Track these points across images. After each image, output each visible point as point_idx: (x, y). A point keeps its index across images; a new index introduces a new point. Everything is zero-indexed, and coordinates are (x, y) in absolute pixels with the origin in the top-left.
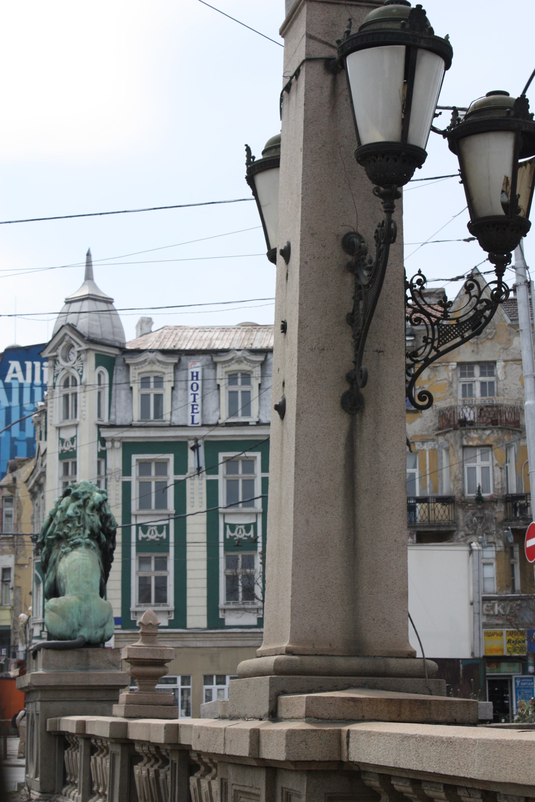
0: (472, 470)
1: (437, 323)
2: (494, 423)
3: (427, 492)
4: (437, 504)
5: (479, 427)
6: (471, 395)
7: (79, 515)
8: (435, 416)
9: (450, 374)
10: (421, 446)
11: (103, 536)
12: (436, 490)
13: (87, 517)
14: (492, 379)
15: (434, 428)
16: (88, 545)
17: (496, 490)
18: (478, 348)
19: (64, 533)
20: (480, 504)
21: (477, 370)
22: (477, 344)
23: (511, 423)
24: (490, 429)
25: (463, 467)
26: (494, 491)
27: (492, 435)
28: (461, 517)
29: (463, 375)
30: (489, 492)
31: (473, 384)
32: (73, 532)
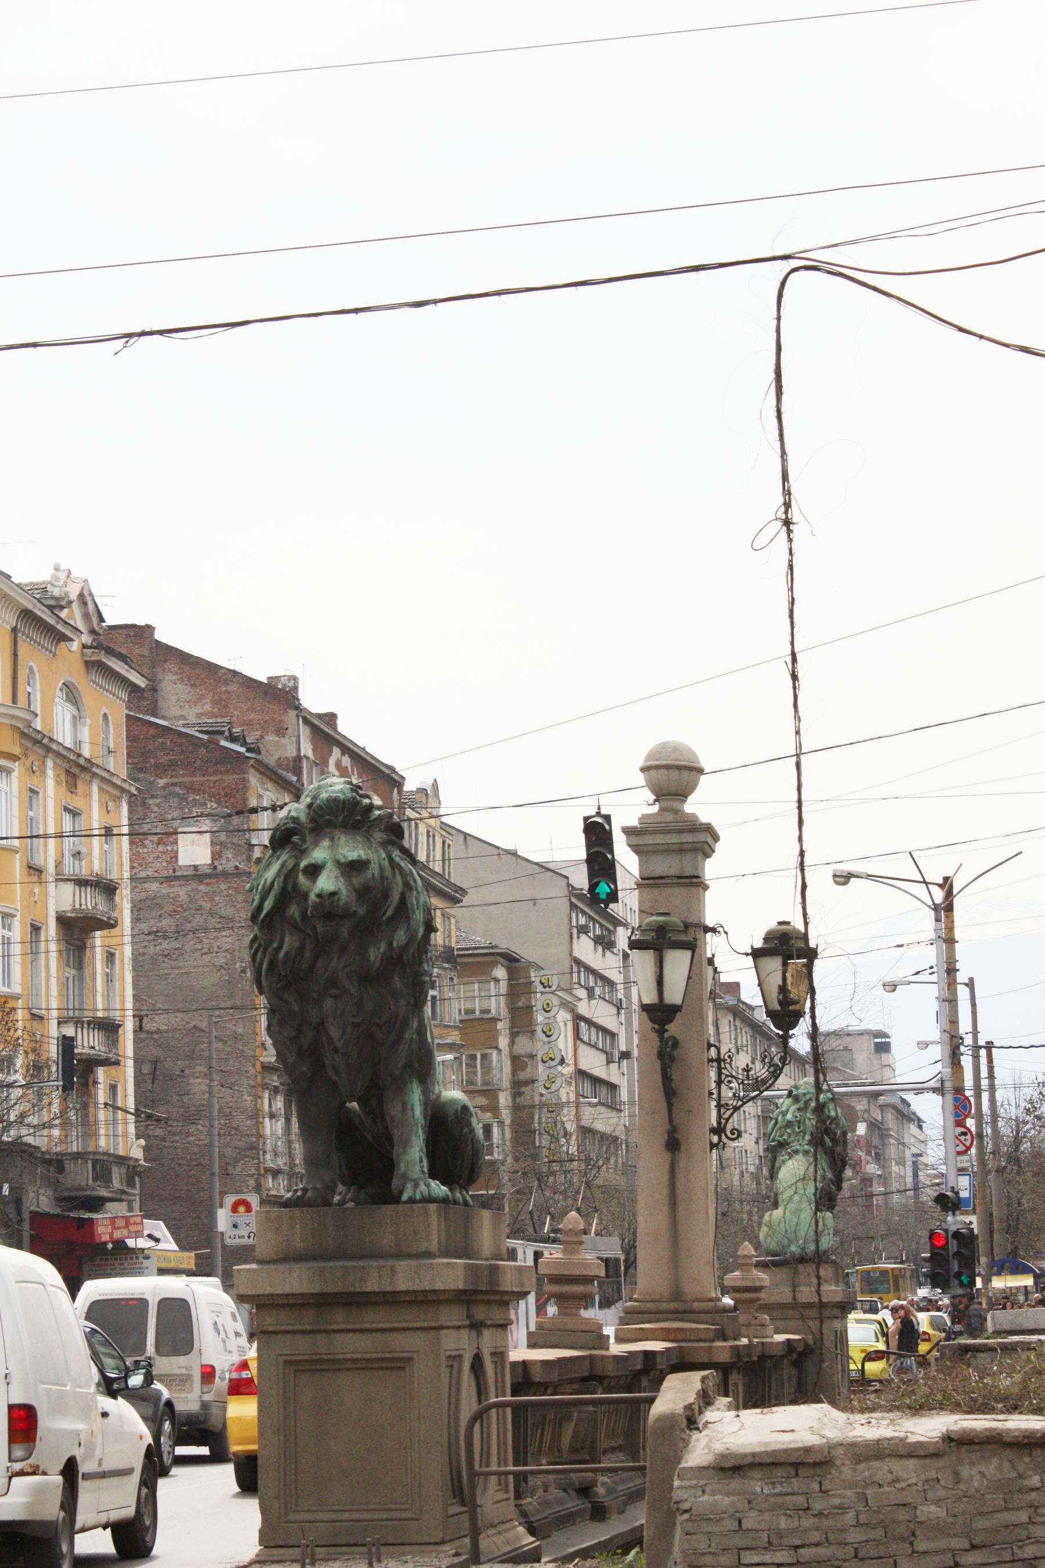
1: (742, 1083)
11: (827, 1140)
13: (807, 1121)
16: (806, 1153)
32: (792, 1138)
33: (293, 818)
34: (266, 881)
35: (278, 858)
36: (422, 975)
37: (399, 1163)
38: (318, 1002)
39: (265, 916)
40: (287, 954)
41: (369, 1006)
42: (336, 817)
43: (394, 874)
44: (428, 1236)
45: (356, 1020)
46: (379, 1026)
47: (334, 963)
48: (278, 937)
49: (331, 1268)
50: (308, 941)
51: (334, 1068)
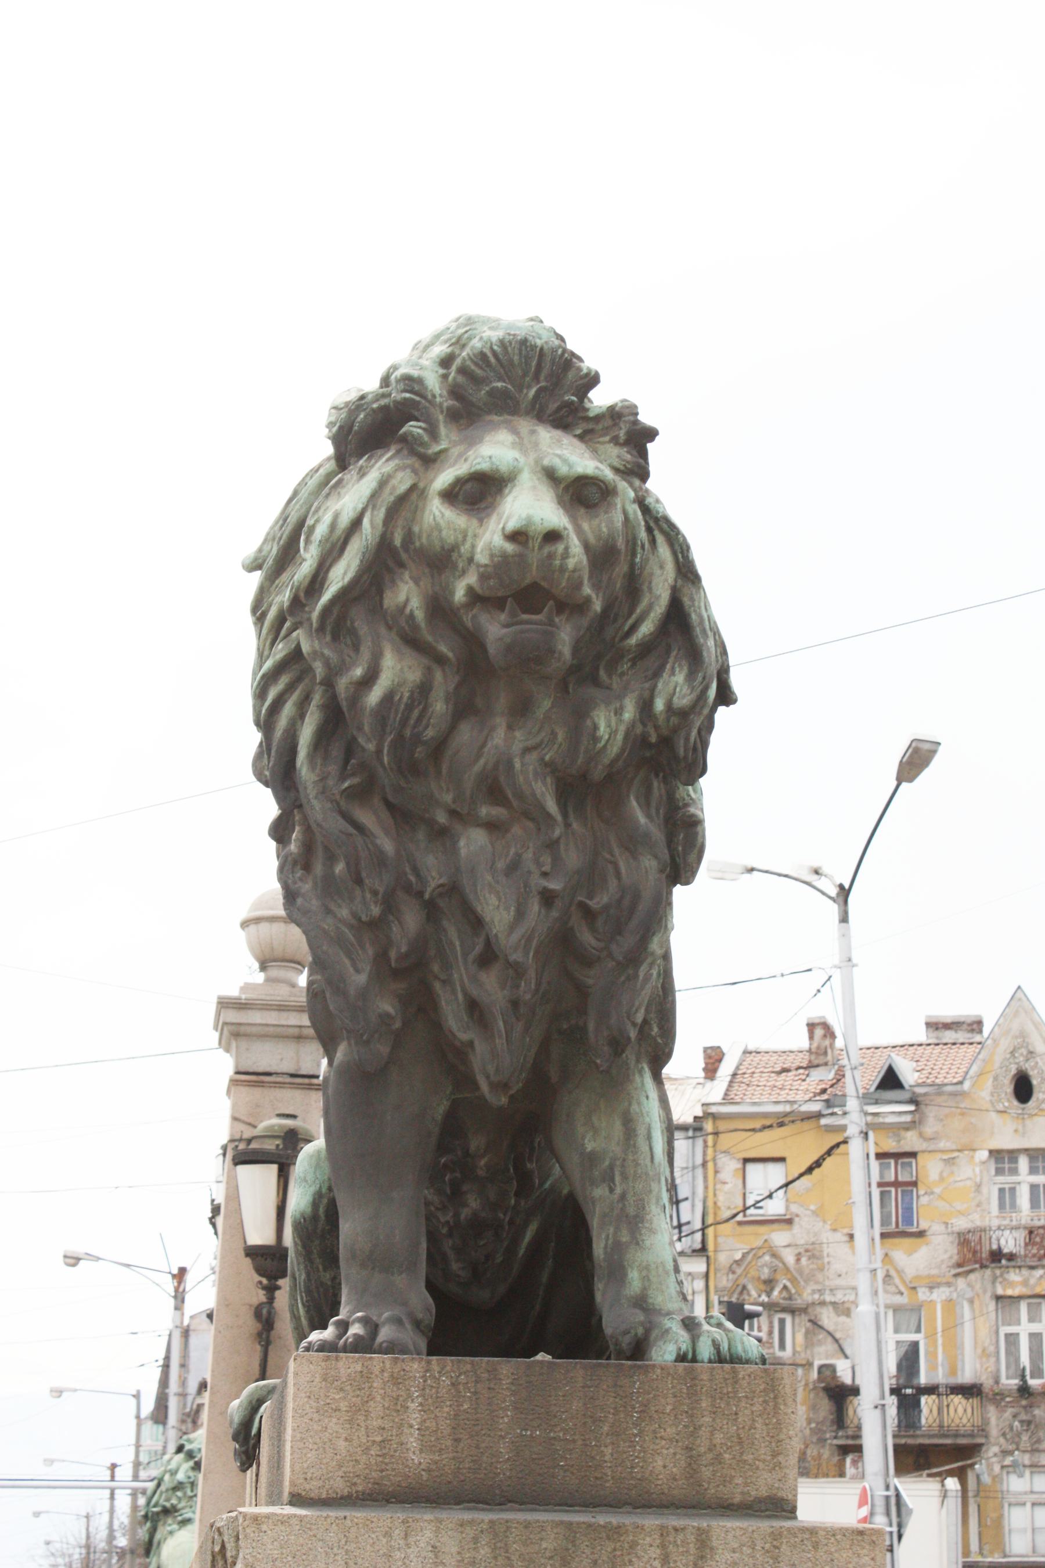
0: (1012, 1340)
3: (938, 1376)
4: (952, 1396)
5: (1023, 1263)
6: (1013, 1205)
7: (191, 1480)
8: (952, 1243)
9: (977, 1170)
10: (928, 1294)
12: (953, 1371)
15: (950, 1264)
18: (1024, 1126)
19: (172, 1504)
20: (1026, 1399)
21: (1023, 1163)
25: (997, 1332)
28: (993, 1421)
29: (999, 1172)
33: (407, 379)
34: (336, 516)
35: (362, 473)
36: (686, 805)
37: (618, 1272)
38: (441, 835)
39: (333, 602)
40: (388, 698)
41: (573, 858)
42: (520, 388)
43: (653, 541)
44: (775, 1454)
45: (555, 885)
46: (589, 915)
47: (499, 737)
48: (365, 654)
49: (527, 1525)
50: (438, 676)
51: (474, 1008)
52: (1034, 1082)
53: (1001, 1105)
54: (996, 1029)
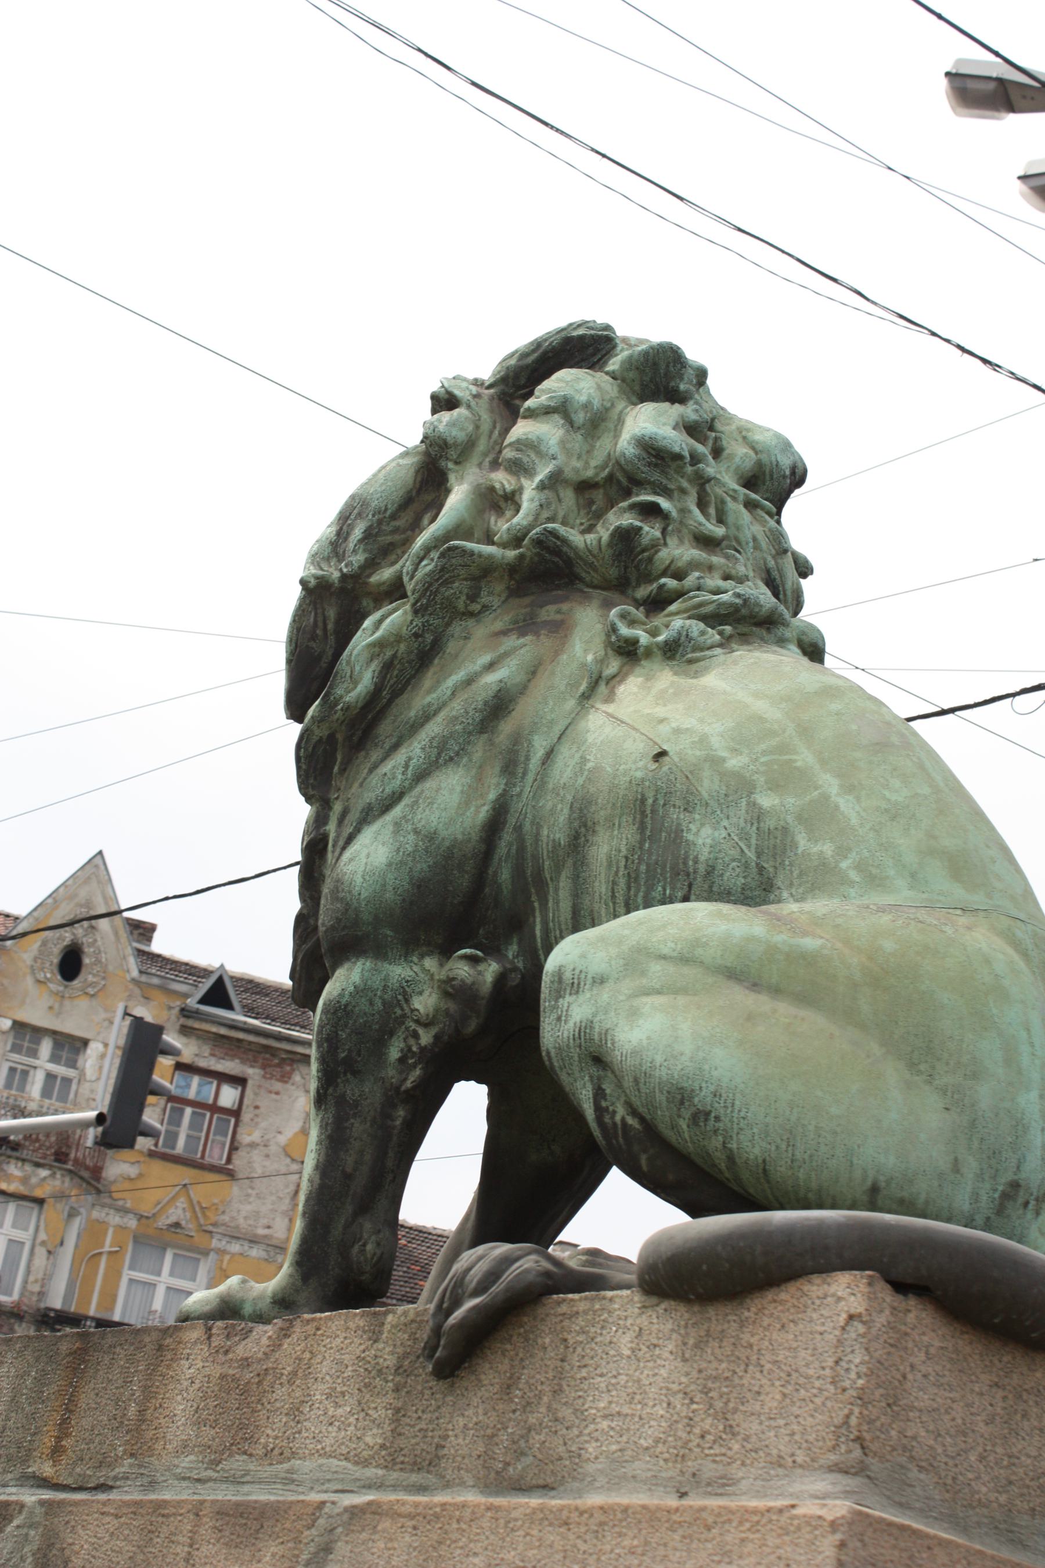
2: (61, 1157)
5: (28, 1157)
14: (70, 1073)
17: (27, 1294)
18: (61, 1005)
21: (46, 1047)
22: (63, 997)
23: (87, 1168)
24: (51, 1167)
26: (22, 1295)
27: (50, 1181)
29: (16, 1048)
30: (10, 1295)
31: (32, 1072)
52: (86, 961)
53: (42, 975)
54: (61, 890)
